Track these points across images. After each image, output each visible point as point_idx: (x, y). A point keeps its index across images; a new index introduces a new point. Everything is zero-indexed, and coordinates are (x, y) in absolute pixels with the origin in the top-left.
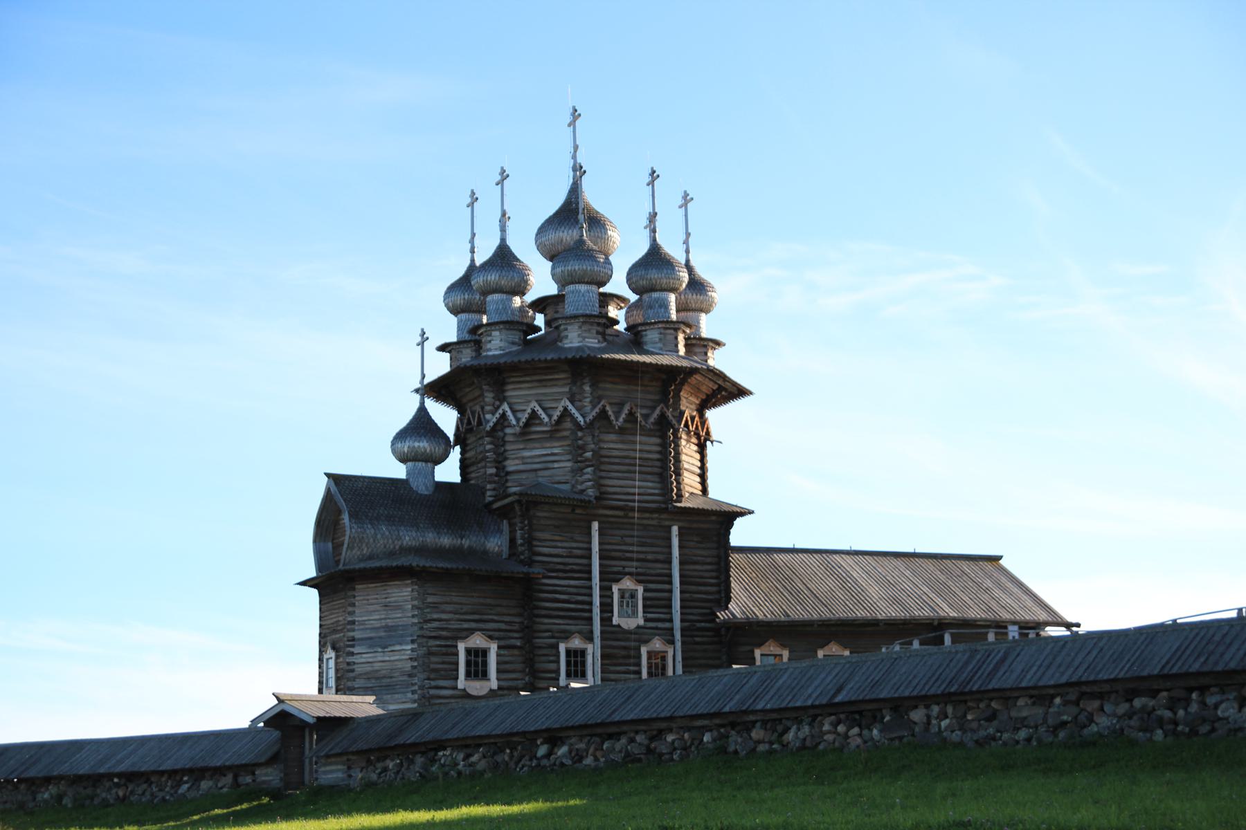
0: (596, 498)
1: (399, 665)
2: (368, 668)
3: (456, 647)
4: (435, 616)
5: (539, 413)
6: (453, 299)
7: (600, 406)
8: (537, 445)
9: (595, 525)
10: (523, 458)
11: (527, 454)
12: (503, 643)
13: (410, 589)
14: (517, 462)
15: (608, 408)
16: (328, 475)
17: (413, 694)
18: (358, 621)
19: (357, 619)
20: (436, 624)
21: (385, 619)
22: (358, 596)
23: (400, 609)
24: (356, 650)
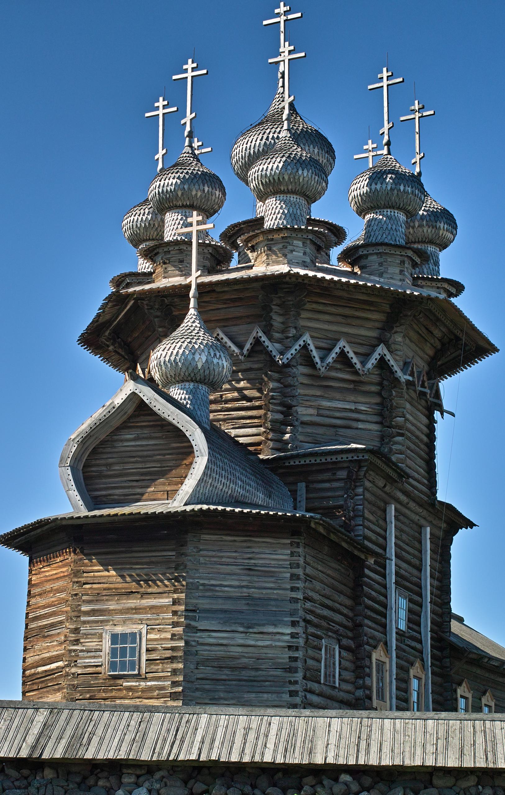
1: (271, 653)
2: (219, 652)
8: (338, 395)
10: (318, 408)
11: (326, 404)
13: (289, 552)
17: (291, 696)
18: (203, 585)
19: (202, 582)
21: (247, 587)
23: (272, 577)
24: (202, 625)
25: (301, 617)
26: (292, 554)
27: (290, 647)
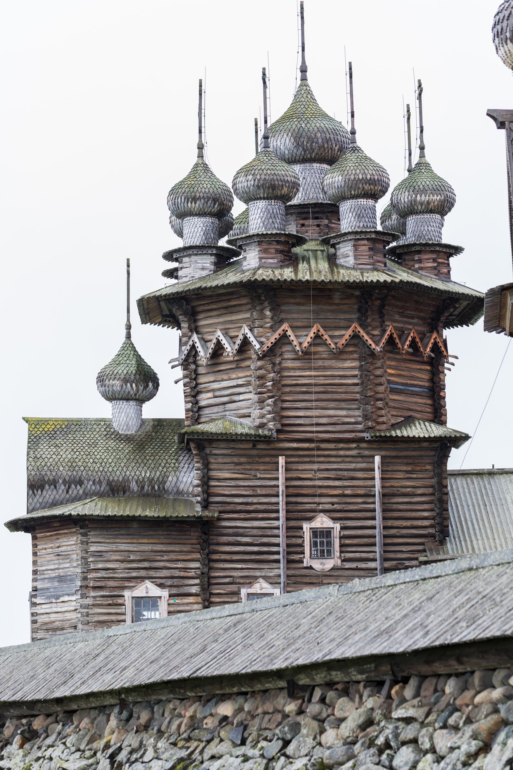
0: (278, 431)
1: (69, 616)
5: (223, 342)
7: (280, 331)
8: (225, 377)
9: (282, 460)
10: (213, 390)
12: (174, 591)
14: (210, 395)
15: (290, 332)
16: (26, 420)
21: (58, 569)
22: (40, 545)
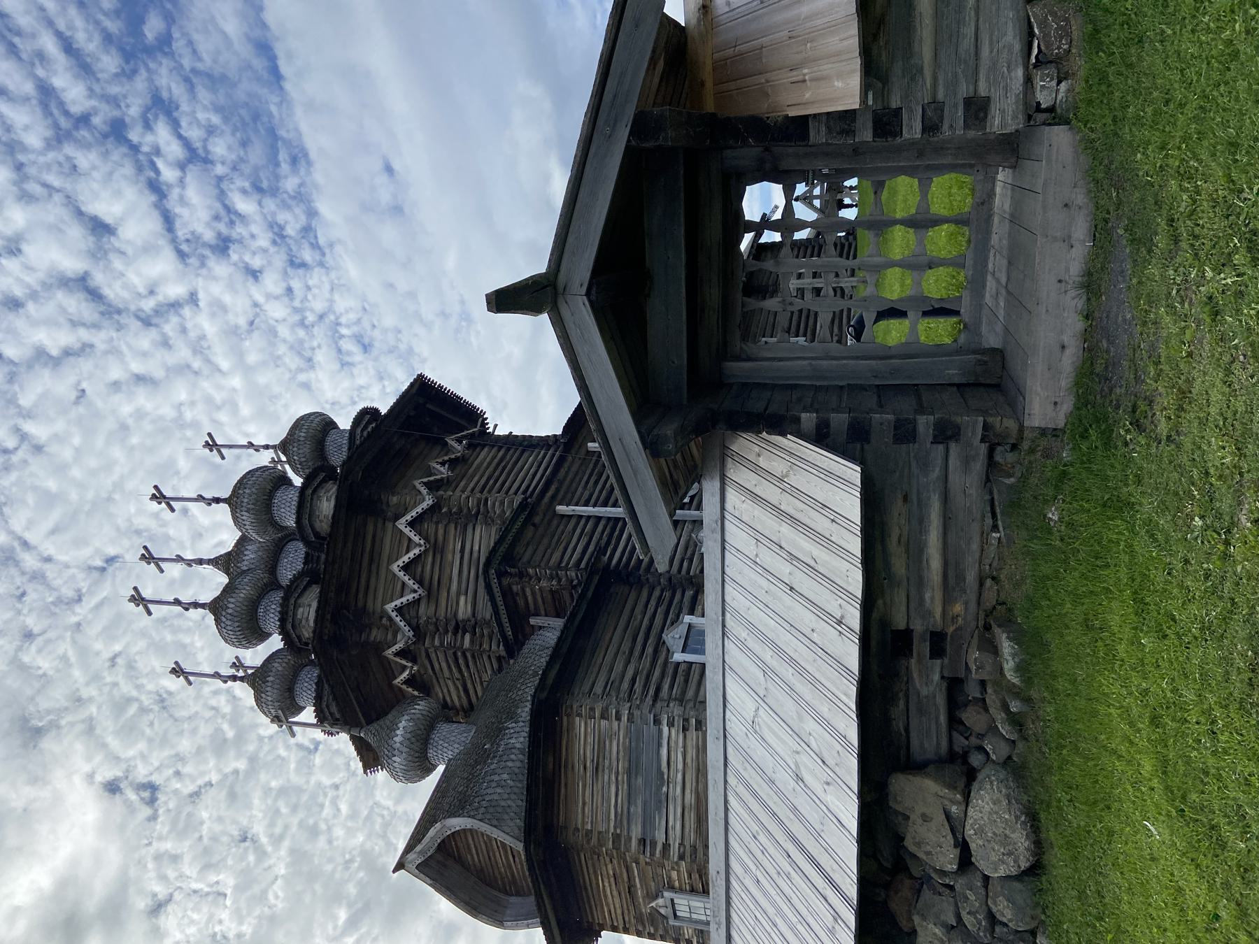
3: (678, 664)
4: (625, 685)
6: (270, 699)
9: (561, 509)
10: (458, 594)
12: (685, 610)
13: (577, 719)
18: (615, 828)
19: (612, 830)
20: (638, 687)
21: (617, 773)
25: (650, 712)
26: (580, 715)
27: (685, 729)
